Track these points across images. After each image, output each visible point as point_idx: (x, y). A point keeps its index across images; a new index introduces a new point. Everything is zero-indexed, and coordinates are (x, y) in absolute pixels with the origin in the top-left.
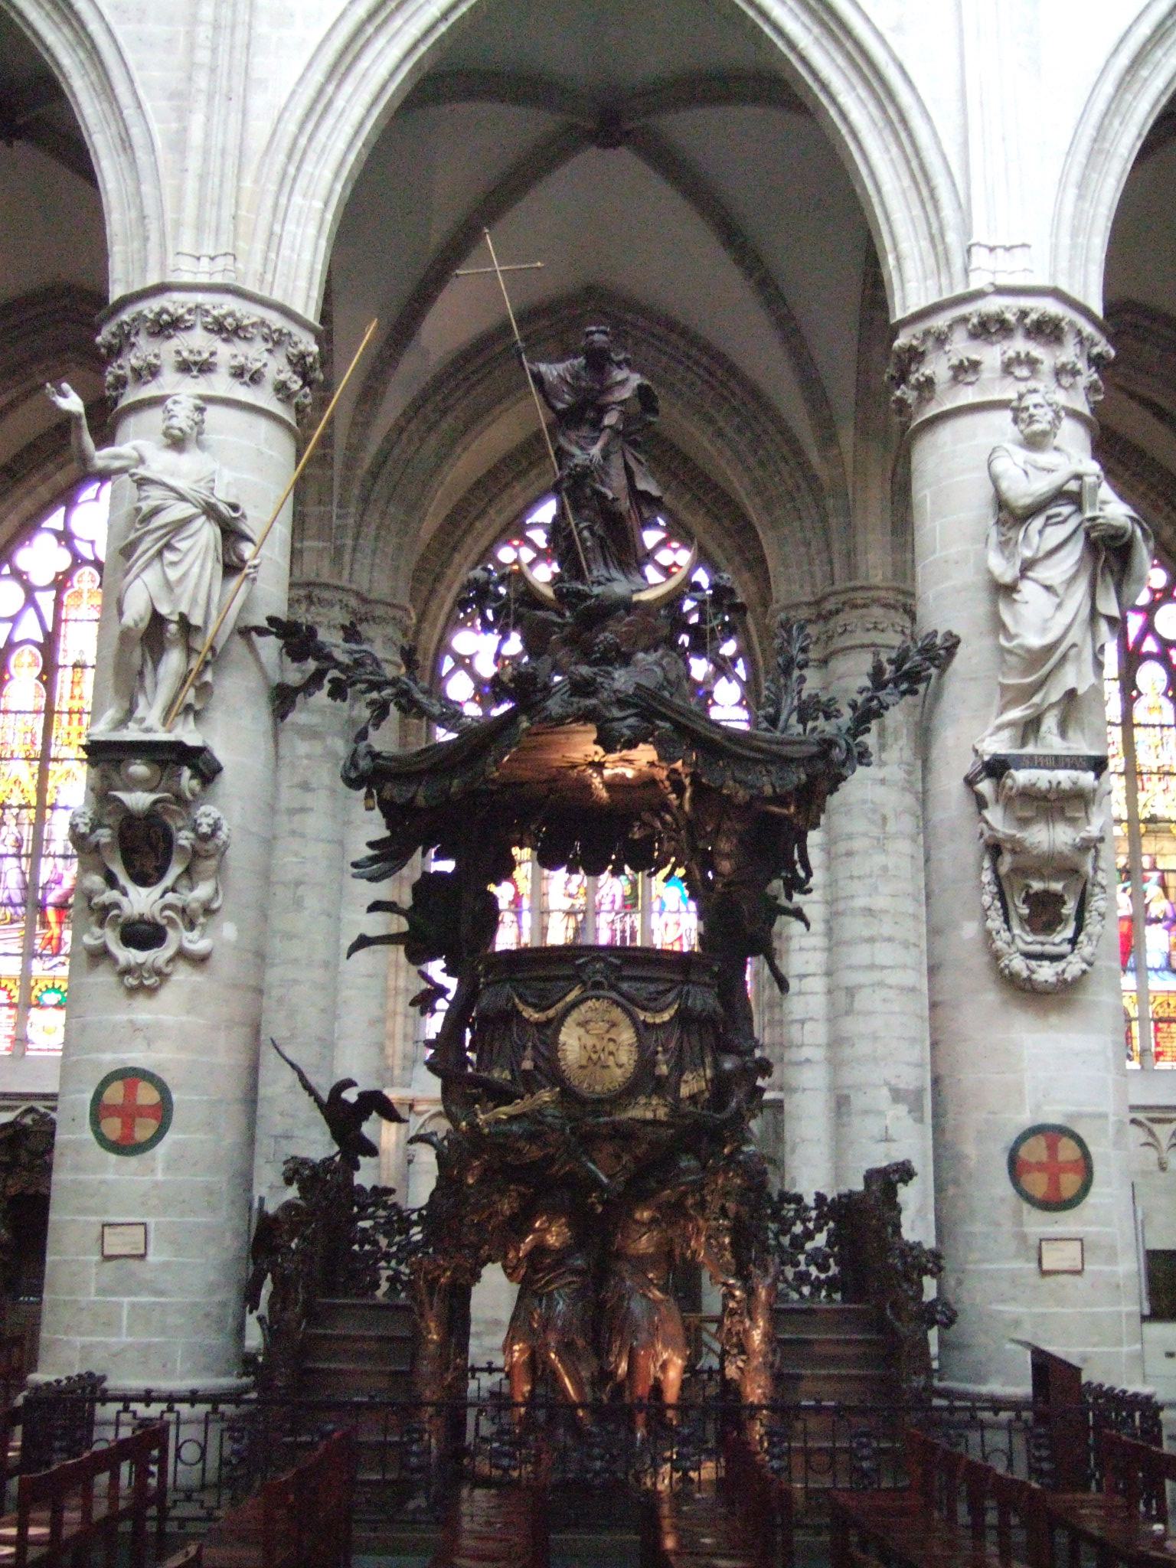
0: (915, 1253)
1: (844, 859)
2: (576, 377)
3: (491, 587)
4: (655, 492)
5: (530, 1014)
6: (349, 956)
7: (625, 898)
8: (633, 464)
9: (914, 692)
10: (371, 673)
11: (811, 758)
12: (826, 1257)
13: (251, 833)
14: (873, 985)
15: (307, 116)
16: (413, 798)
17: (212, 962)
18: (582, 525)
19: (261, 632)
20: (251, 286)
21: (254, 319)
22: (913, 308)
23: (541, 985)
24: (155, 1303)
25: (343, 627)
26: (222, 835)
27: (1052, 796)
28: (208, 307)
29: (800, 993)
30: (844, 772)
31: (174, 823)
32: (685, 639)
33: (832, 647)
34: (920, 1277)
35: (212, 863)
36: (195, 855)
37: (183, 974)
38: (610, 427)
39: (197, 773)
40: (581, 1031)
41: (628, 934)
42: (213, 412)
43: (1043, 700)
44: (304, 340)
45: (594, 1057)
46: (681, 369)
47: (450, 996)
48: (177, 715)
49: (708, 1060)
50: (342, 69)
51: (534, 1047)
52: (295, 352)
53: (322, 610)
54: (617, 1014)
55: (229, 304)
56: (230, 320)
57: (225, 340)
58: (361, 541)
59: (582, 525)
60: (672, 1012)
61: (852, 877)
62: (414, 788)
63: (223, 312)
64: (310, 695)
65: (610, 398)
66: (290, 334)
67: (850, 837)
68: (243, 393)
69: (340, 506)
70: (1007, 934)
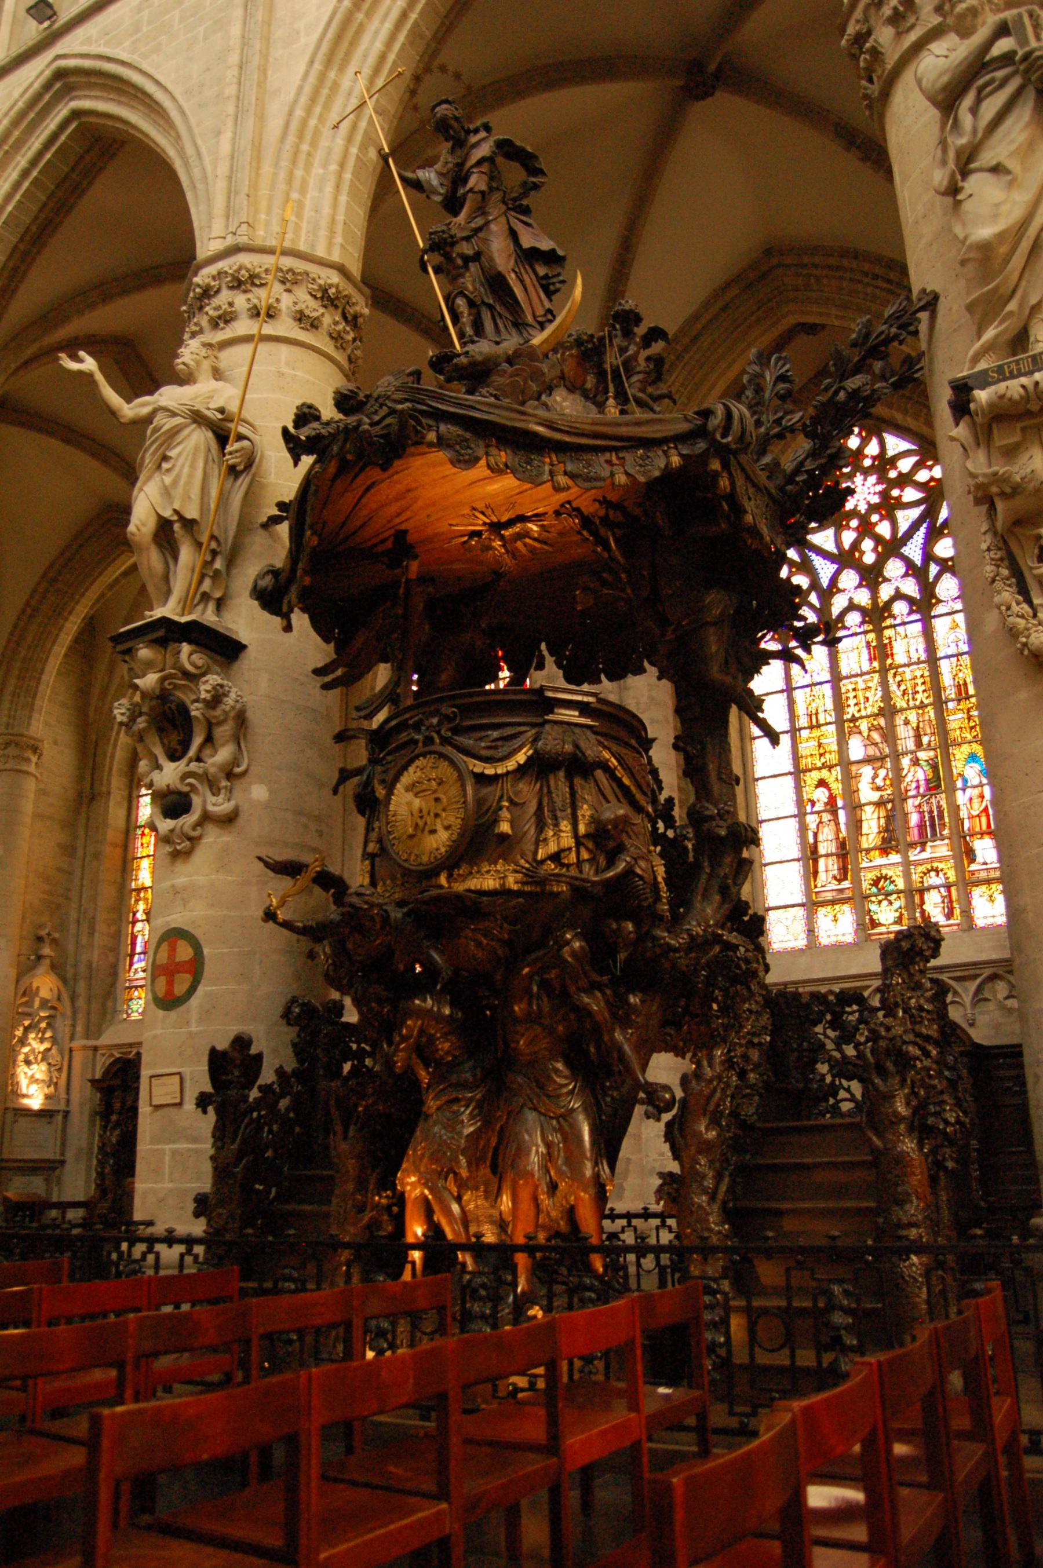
7: (927, 781)
8: (519, 227)
15: (313, 100)
17: (241, 821)
24: (189, 1150)
26: (229, 701)
27: (1034, 407)
31: (186, 698)
37: (213, 838)
40: (409, 796)
43: (1021, 305)
44: (323, 275)
45: (421, 823)
46: (860, 287)
50: (340, 54)
52: (316, 287)
56: (243, 272)
60: (521, 758)
63: (235, 268)
70: (1025, 606)
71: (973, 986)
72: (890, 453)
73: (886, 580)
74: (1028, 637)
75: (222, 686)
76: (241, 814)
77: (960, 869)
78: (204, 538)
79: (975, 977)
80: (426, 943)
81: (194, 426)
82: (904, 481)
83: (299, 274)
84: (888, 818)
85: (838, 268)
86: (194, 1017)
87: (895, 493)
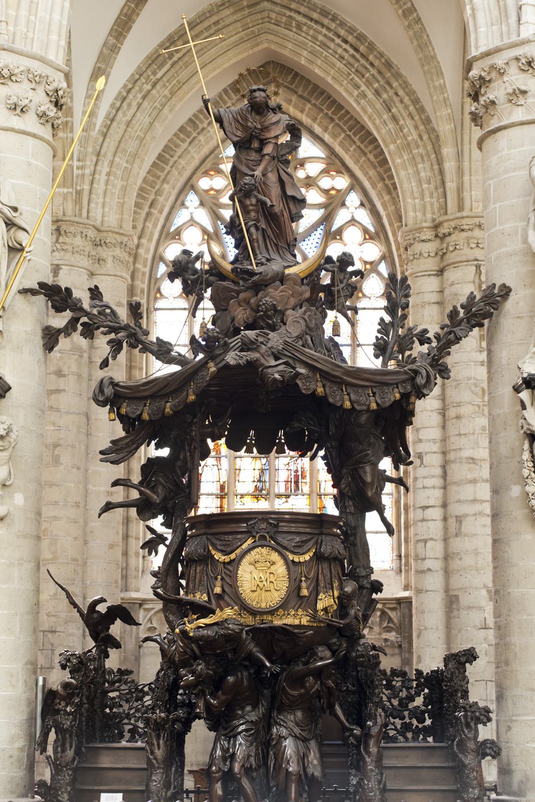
0: (473, 709)
1: (454, 421)
3: (190, 265)
5: (218, 556)
6: (100, 515)
9: (481, 325)
11: (404, 381)
12: (423, 712)
14: (475, 515)
16: (141, 414)
18: (250, 224)
19: (33, 292)
21: (22, 69)
22: (483, 49)
25: (90, 289)
26: (13, 435)
29: (423, 520)
30: (425, 392)
32: (322, 295)
33: (445, 263)
34: (476, 725)
38: (268, 154)
40: (252, 567)
41: (299, 473)
45: (261, 585)
46: (332, 45)
47: (167, 542)
49: (336, 584)
51: (222, 579)
53: (67, 240)
54: (275, 556)
58: (95, 185)
60: (311, 554)
61: (460, 435)
64: (69, 335)
65: (268, 135)
67: (459, 405)
69: (79, 160)
80: (254, 649)
84: (262, 471)
85: (317, 22)
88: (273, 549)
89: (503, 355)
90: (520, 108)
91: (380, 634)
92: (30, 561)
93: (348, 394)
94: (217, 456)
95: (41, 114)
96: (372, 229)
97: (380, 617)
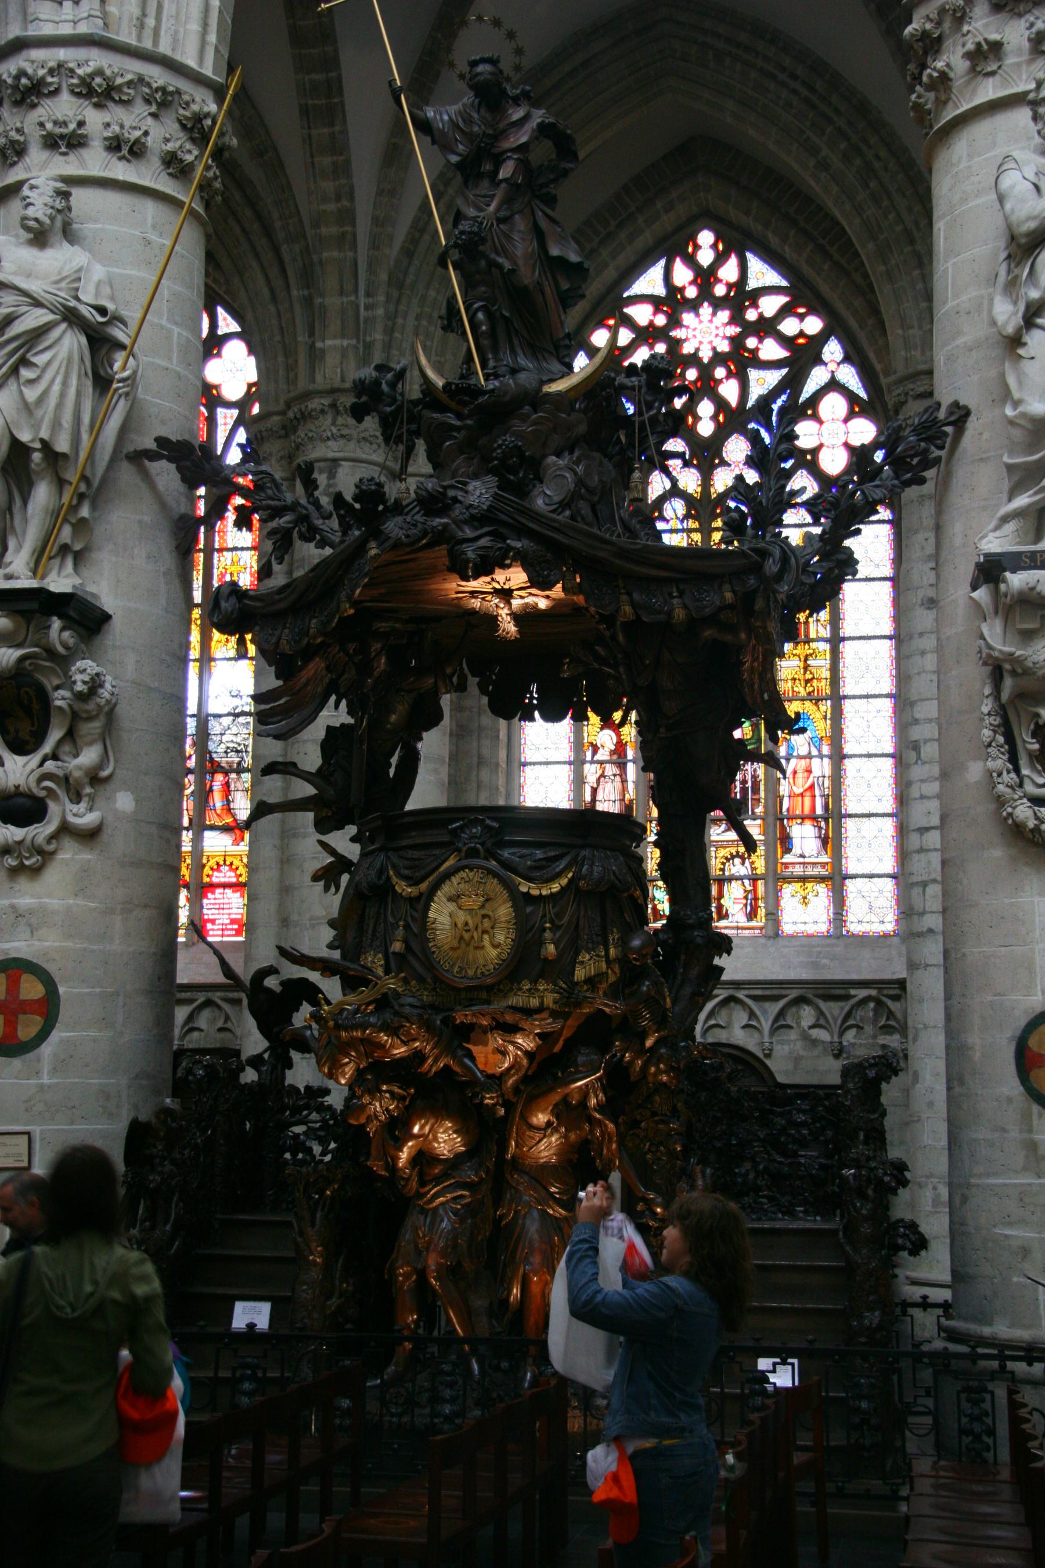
2: (469, 121)
4: (574, 258)
5: (403, 888)
8: (543, 223)
10: (273, 499)
13: (151, 689)
17: (105, 836)
19: (151, 456)
20: (126, 36)
21: (129, 77)
23: (416, 854)
26: (105, 693)
28: (71, 65)
31: (49, 682)
35: (96, 726)
36: (75, 719)
37: (69, 853)
38: (506, 180)
39: (69, 624)
40: (452, 907)
41: (749, 784)
42: (80, 196)
44: (198, 99)
45: (466, 936)
48: (50, 558)
49: (614, 936)
51: (407, 927)
52: (188, 114)
54: (493, 885)
55: (96, 59)
56: (98, 80)
57: (98, 106)
59: (476, 306)
60: (564, 881)
62: (277, 633)
63: (89, 70)
66: (178, 92)
68: (122, 171)
69: (368, 295)
70: (1013, 775)
71: (774, 1008)
72: (752, 284)
73: (724, 463)
74: (1014, 808)
75: (98, 675)
76: (105, 827)
77: (771, 860)
78: (72, 475)
79: (776, 998)
81: (64, 326)
82: (766, 327)
83: (172, 93)
86: (46, 1067)
87: (751, 342)
88: (490, 872)
89: (956, 529)
90: (991, 80)
91: (875, 1037)
92: (146, 906)
93: (629, 594)
94: (620, 760)
95: (168, 159)
96: (863, 394)
97: (875, 1010)
